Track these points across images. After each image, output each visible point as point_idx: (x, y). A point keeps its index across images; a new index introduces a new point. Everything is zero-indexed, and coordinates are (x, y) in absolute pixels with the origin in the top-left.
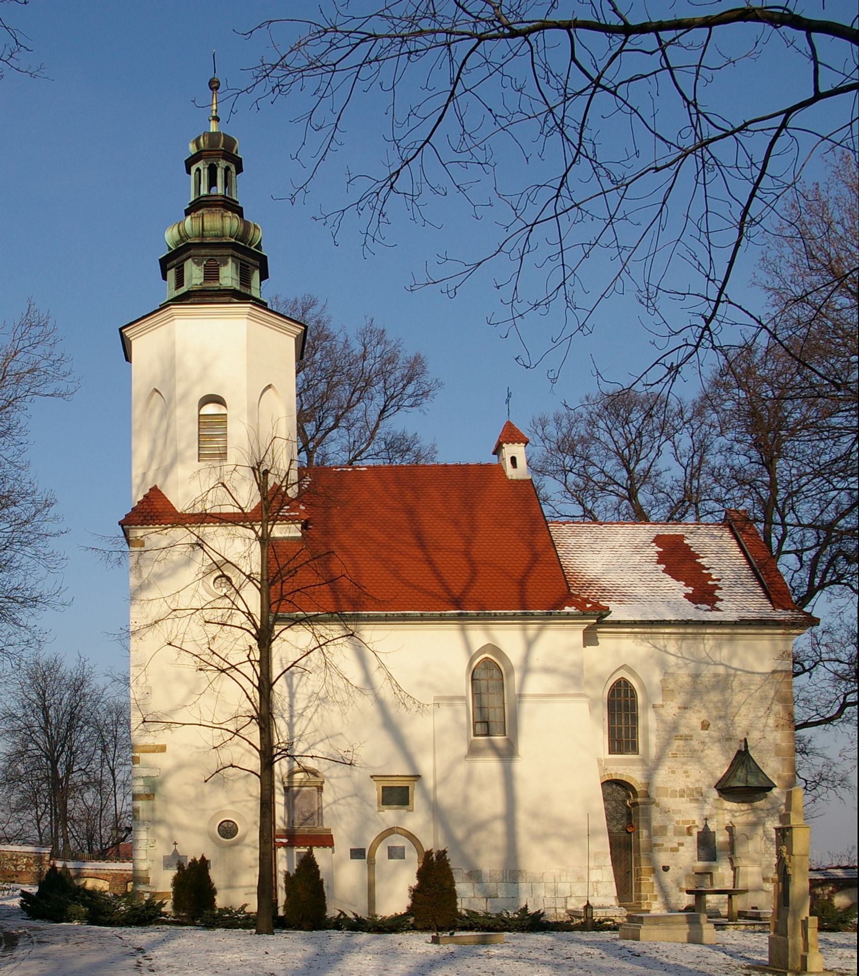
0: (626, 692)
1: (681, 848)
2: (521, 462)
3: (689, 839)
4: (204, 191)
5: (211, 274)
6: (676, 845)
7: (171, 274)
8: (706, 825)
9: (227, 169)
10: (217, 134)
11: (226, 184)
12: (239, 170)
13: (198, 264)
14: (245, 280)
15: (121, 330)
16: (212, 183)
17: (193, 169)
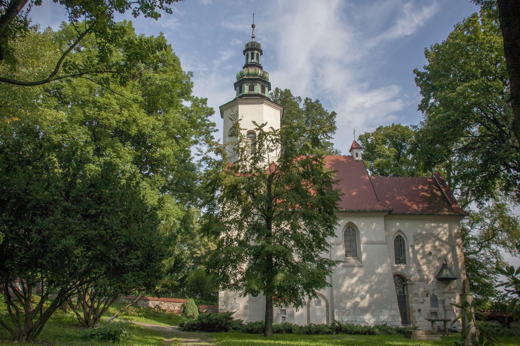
0: (400, 240)
1: (425, 302)
2: (359, 154)
3: (427, 298)
4: (249, 61)
5: (251, 88)
6: (422, 301)
7: (238, 88)
8: (433, 293)
9: (257, 54)
10: (255, 42)
11: (258, 58)
12: (261, 54)
13: (247, 85)
14: (263, 91)
15: (220, 107)
16: (252, 58)
17: (246, 54)
